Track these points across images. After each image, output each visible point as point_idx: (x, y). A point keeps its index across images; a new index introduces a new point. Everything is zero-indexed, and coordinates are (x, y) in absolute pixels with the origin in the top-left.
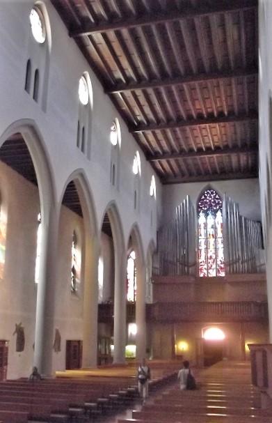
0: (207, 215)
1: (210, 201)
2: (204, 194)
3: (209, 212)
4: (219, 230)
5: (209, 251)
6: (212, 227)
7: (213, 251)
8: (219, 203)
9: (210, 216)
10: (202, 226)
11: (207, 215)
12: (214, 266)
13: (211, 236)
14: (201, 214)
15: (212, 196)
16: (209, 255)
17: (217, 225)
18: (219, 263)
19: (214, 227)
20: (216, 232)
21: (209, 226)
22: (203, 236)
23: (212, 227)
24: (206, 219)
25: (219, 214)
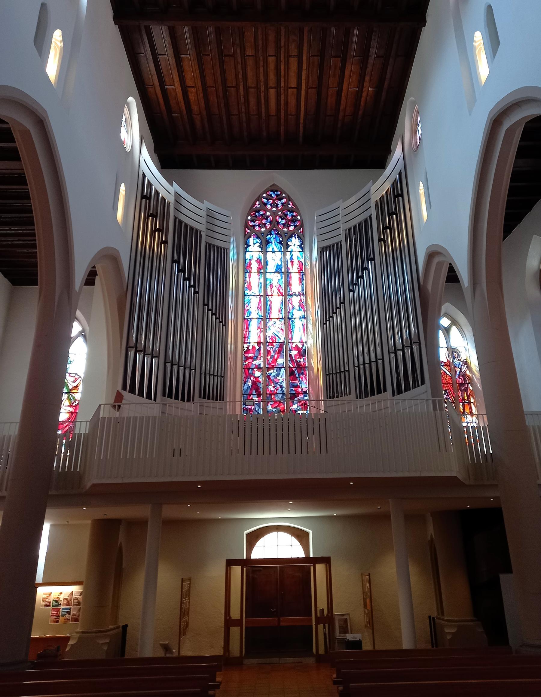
0: (265, 244)
1: (274, 214)
2: (259, 198)
3: (272, 238)
4: (295, 278)
5: (270, 323)
6: (278, 270)
7: (280, 324)
8: (294, 220)
9: (274, 246)
10: (254, 266)
11: (265, 244)
12: (280, 361)
13: (275, 291)
14: (251, 241)
15: (279, 202)
16: (269, 334)
17: (290, 265)
18: (294, 353)
19: (283, 271)
20: (288, 283)
21: (271, 268)
22: (255, 290)
23: (278, 270)
24: (265, 252)
25: (295, 242)
